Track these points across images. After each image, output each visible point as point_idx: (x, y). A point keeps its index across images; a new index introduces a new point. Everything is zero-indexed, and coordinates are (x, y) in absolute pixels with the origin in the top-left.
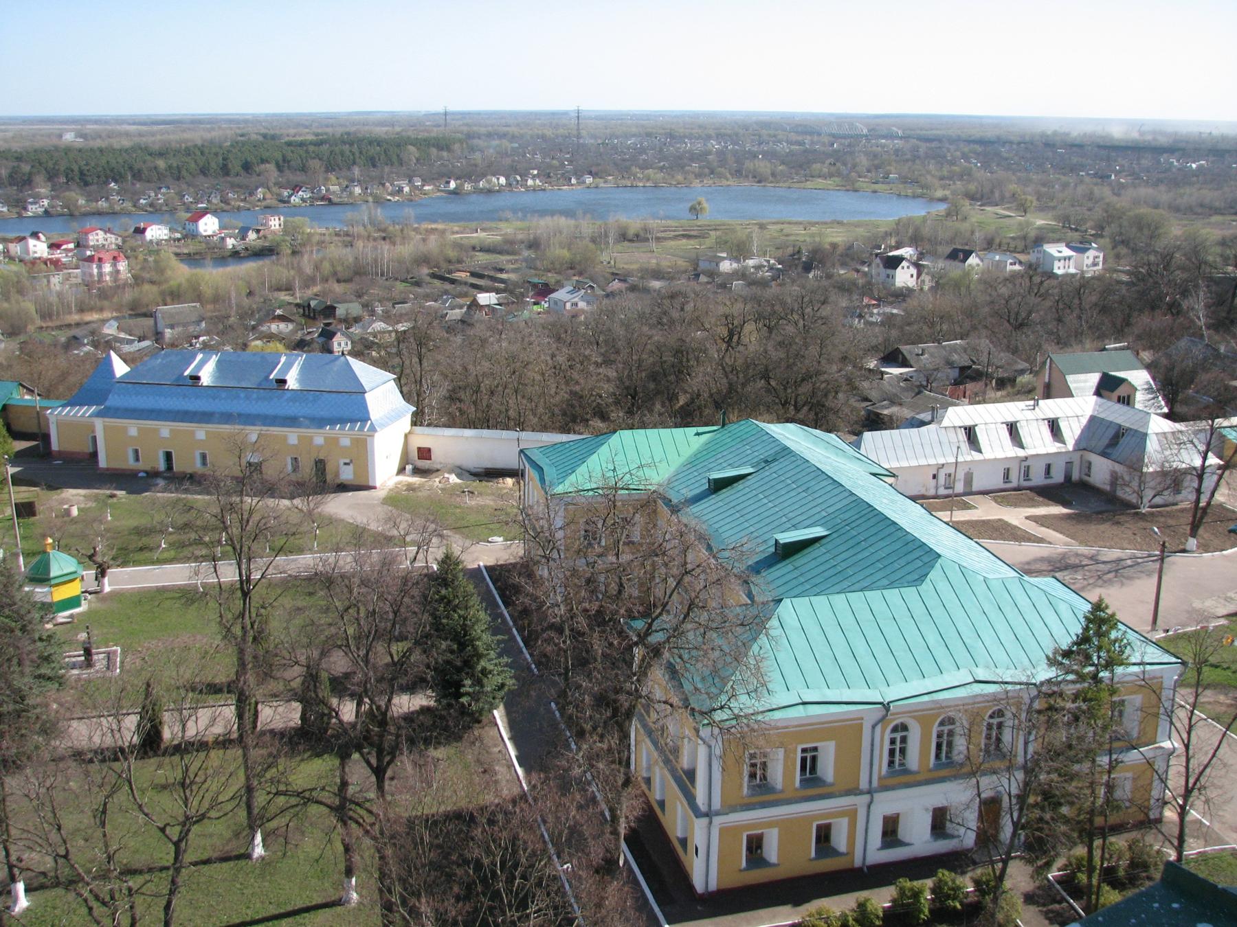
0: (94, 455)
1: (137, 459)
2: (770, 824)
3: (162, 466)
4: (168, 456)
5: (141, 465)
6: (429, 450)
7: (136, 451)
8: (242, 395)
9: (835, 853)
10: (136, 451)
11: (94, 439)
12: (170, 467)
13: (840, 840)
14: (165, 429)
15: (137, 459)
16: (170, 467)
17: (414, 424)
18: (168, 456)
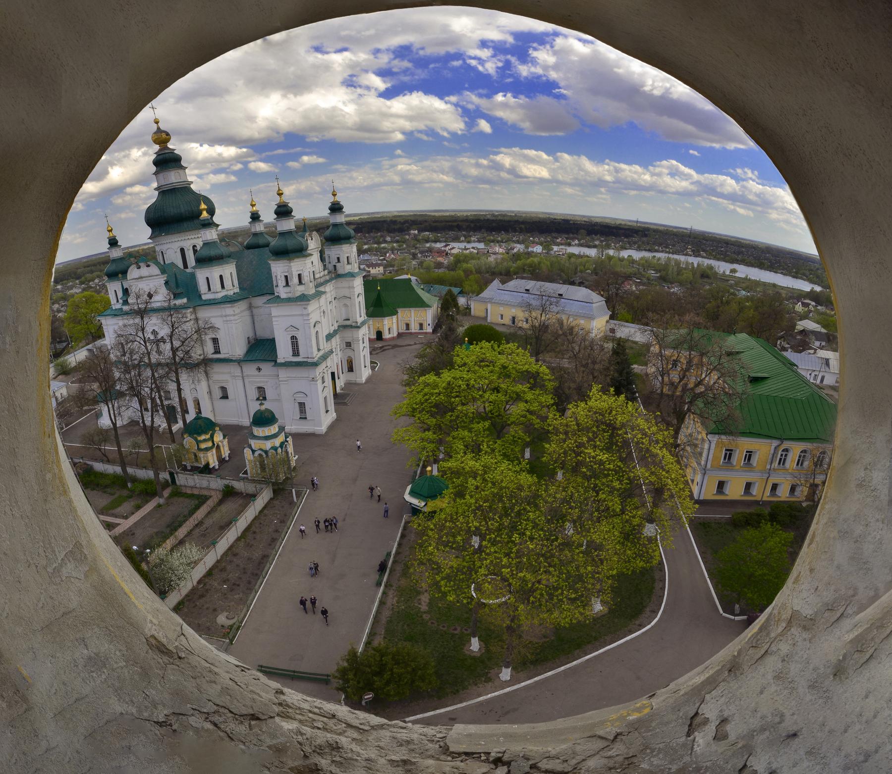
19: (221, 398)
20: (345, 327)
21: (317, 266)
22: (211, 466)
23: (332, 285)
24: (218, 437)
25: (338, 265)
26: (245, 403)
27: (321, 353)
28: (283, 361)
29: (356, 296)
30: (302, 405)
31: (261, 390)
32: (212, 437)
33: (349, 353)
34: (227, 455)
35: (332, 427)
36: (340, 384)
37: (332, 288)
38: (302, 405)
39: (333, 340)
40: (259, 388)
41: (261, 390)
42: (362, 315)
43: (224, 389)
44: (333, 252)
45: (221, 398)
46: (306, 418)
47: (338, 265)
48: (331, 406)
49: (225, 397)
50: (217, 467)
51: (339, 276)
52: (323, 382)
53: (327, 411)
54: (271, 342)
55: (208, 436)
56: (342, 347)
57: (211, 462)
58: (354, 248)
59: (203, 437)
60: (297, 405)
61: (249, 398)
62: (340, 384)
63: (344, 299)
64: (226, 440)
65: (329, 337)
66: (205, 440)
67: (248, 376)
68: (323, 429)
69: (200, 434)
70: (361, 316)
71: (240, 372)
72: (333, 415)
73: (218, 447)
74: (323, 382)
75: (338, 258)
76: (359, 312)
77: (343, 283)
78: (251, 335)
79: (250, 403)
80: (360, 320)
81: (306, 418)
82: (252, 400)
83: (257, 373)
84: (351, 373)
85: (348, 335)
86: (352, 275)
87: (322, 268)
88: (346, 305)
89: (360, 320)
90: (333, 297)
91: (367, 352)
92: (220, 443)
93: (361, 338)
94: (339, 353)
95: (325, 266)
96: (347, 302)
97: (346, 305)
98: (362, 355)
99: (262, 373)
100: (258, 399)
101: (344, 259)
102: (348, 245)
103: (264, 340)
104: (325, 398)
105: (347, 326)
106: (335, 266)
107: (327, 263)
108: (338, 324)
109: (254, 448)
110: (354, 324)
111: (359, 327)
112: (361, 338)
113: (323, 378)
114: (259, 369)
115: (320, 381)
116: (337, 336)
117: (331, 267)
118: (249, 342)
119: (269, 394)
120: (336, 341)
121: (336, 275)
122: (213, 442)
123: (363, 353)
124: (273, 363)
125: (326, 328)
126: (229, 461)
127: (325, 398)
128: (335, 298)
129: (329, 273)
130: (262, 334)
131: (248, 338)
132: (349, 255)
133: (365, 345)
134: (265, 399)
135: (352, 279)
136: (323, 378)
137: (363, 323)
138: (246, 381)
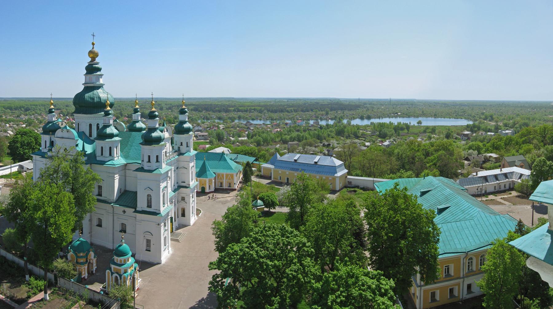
0: (271, 177)
1: (280, 179)
2: (437, 289)
3: (286, 181)
4: (288, 179)
5: (281, 181)
7: (280, 177)
8: (306, 165)
9: (455, 296)
10: (280, 177)
11: (271, 173)
12: (288, 182)
13: (456, 293)
14: (288, 172)
15: (280, 179)
16: (288, 182)
18: (288, 179)
25: (181, 147)
29: (190, 168)
44: (179, 138)
47: (181, 147)
55: (84, 254)
59: (81, 254)
69: (80, 252)
71: (112, 210)
75: (182, 143)
83: (122, 213)
95: (173, 147)
99: (125, 214)
101: (184, 144)
103: (131, 191)
106: (179, 148)
110: (187, 186)
114: (124, 212)
118: (120, 193)
130: (130, 188)
138: (115, 218)
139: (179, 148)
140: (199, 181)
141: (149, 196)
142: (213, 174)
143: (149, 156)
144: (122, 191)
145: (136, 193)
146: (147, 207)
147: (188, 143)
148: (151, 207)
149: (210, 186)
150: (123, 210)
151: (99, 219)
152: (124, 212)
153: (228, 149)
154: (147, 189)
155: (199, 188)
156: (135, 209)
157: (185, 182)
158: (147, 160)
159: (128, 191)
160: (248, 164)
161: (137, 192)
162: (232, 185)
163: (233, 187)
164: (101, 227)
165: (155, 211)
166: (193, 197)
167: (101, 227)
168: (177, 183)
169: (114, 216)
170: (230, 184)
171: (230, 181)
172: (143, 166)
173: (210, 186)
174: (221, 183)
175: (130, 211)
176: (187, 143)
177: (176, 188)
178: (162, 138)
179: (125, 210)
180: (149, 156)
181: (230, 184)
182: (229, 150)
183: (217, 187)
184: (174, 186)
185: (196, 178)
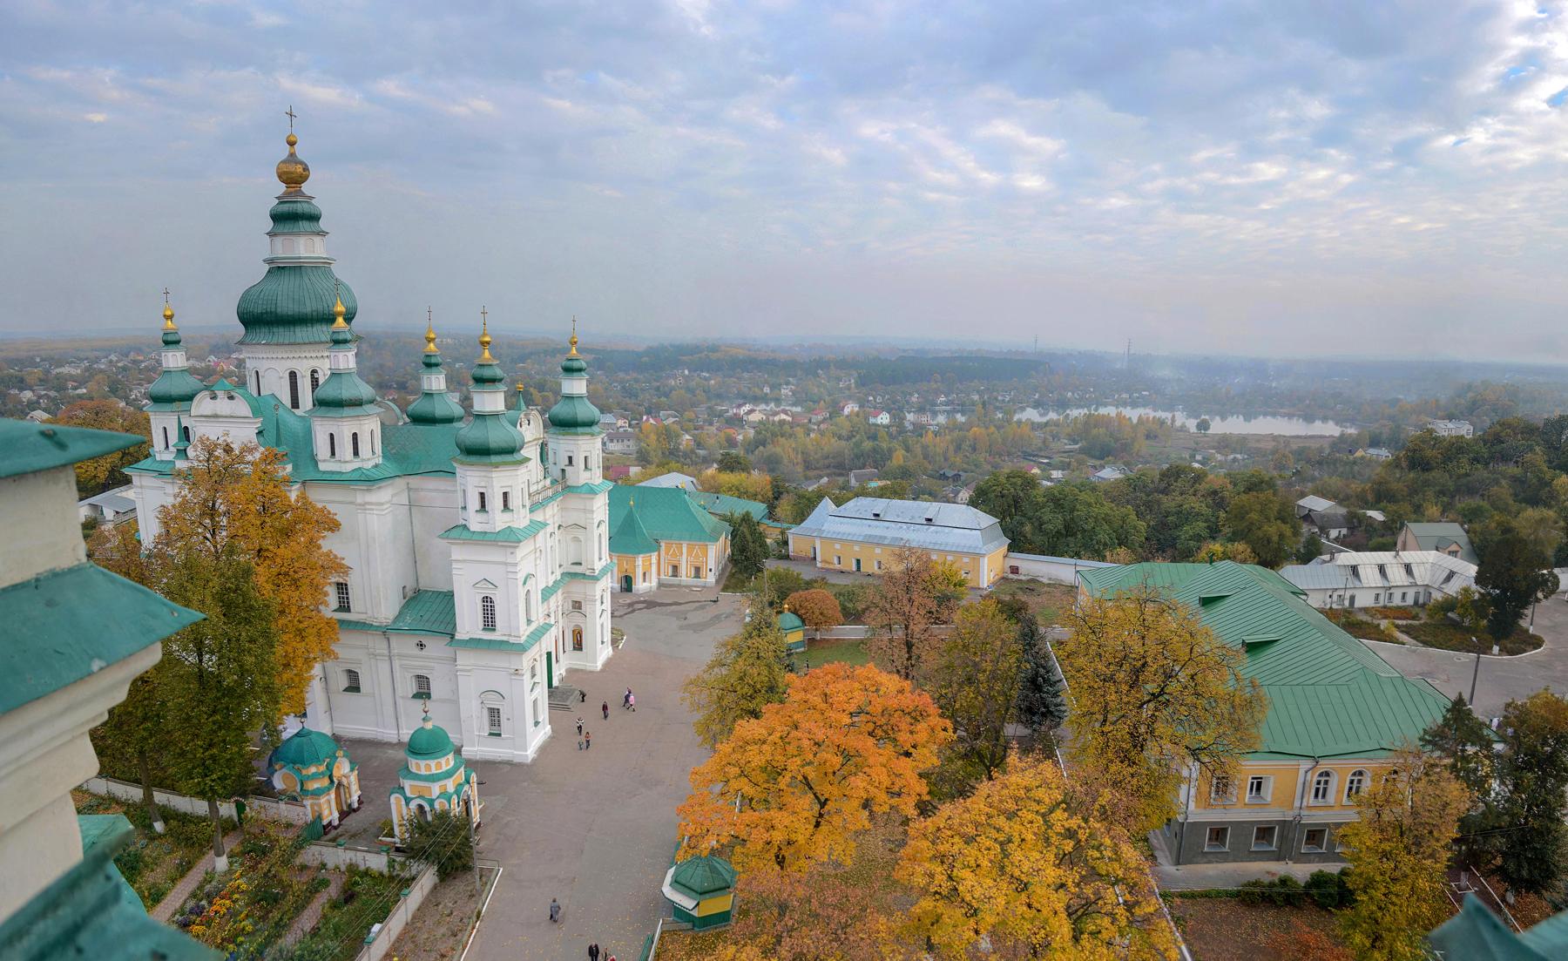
6: (1017, 568)
17: (1008, 550)
19: (346, 690)
20: (575, 575)
21: (534, 471)
22: (325, 822)
23: (556, 505)
24: (343, 768)
26: (391, 702)
27: (533, 626)
28: (466, 637)
29: (596, 525)
30: (494, 714)
31: (422, 681)
32: (329, 768)
33: (577, 619)
34: (355, 798)
35: (543, 750)
36: (559, 671)
37: (556, 509)
38: (494, 714)
39: (553, 600)
40: (419, 677)
41: (422, 681)
42: (603, 557)
43: (353, 675)
44: (563, 445)
45: (346, 690)
46: (499, 735)
48: (544, 715)
49: (354, 687)
50: (336, 823)
51: (568, 489)
52: (533, 676)
53: (537, 723)
54: (447, 598)
56: (566, 607)
57: (326, 812)
58: (598, 443)
60: (486, 713)
61: (399, 692)
62: (559, 671)
63: (575, 529)
64: (356, 772)
65: (547, 593)
66: (314, 777)
67: (400, 656)
68: (530, 753)
70: (600, 559)
72: (545, 730)
73: (340, 784)
74: (533, 676)
76: (599, 556)
77: (574, 502)
78: (410, 585)
79: (400, 702)
80: (598, 566)
81: (499, 735)
82: (402, 697)
83: (416, 651)
84: (578, 653)
85: (578, 591)
86: (592, 491)
87: (541, 475)
88: (577, 540)
89: (598, 566)
90: (557, 525)
91: (607, 620)
92: (345, 781)
93: (598, 597)
94: (561, 621)
96: (580, 534)
97: (577, 540)
98: (598, 622)
99: (423, 653)
100: (417, 696)
102: (588, 437)
104: (535, 702)
105: (576, 575)
107: (550, 466)
108: (562, 570)
109: (408, 794)
110: (588, 573)
111: (595, 579)
112: (598, 597)
113: (533, 668)
114: (421, 645)
115: (527, 676)
116: (560, 592)
117: (556, 473)
118: (404, 598)
119: (436, 689)
120: (557, 600)
121: (562, 486)
122: (331, 778)
123: (599, 623)
124: (448, 638)
125: (545, 579)
126: (358, 809)
127: (535, 702)
128: (560, 526)
129: (554, 482)
131: (404, 587)
132: (588, 454)
133: (604, 607)
134: (428, 696)
135: (592, 496)
136: (533, 668)
137: (604, 571)
138: (396, 664)
139: (563, 470)
140: (615, 561)
141: (485, 599)
142: (654, 542)
143: (482, 495)
144: (410, 594)
145: (450, 595)
146: (484, 629)
147: (589, 460)
148: (494, 630)
149: (645, 574)
150: (417, 642)
151: (350, 671)
152: (421, 645)
153: (692, 479)
154: (482, 583)
155: (616, 578)
156: (453, 636)
157: (580, 564)
158: (477, 506)
159: (427, 591)
160: (746, 518)
161: (452, 592)
162: (703, 573)
163: (706, 578)
164: (359, 692)
165: (505, 638)
166: (602, 603)
167: (359, 692)
168: (560, 566)
169: (393, 662)
170: (697, 570)
171: (698, 564)
172: (464, 522)
173: (645, 574)
174: (675, 568)
175: (436, 647)
176: (586, 457)
177: (559, 578)
178: (518, 445)
179: (424, 643)
180: (482, 495)
181: (697, 570)
182: (695, 481)
183: (662, 577)
184: (552, 573)
185: (610, 555)
